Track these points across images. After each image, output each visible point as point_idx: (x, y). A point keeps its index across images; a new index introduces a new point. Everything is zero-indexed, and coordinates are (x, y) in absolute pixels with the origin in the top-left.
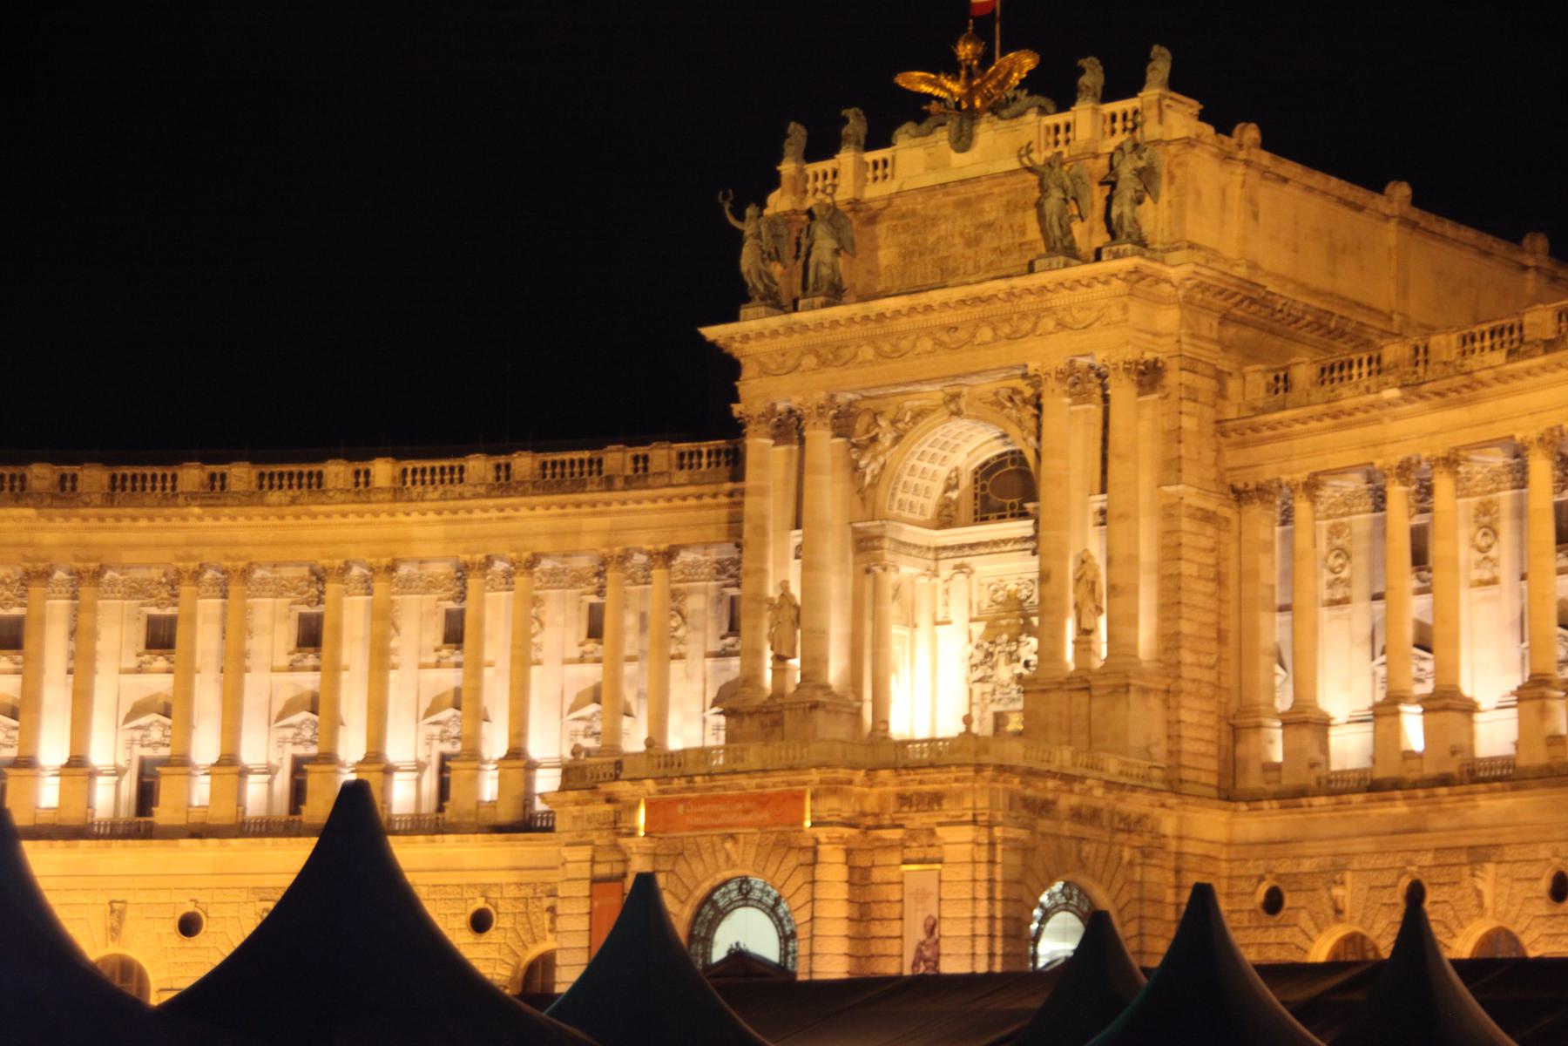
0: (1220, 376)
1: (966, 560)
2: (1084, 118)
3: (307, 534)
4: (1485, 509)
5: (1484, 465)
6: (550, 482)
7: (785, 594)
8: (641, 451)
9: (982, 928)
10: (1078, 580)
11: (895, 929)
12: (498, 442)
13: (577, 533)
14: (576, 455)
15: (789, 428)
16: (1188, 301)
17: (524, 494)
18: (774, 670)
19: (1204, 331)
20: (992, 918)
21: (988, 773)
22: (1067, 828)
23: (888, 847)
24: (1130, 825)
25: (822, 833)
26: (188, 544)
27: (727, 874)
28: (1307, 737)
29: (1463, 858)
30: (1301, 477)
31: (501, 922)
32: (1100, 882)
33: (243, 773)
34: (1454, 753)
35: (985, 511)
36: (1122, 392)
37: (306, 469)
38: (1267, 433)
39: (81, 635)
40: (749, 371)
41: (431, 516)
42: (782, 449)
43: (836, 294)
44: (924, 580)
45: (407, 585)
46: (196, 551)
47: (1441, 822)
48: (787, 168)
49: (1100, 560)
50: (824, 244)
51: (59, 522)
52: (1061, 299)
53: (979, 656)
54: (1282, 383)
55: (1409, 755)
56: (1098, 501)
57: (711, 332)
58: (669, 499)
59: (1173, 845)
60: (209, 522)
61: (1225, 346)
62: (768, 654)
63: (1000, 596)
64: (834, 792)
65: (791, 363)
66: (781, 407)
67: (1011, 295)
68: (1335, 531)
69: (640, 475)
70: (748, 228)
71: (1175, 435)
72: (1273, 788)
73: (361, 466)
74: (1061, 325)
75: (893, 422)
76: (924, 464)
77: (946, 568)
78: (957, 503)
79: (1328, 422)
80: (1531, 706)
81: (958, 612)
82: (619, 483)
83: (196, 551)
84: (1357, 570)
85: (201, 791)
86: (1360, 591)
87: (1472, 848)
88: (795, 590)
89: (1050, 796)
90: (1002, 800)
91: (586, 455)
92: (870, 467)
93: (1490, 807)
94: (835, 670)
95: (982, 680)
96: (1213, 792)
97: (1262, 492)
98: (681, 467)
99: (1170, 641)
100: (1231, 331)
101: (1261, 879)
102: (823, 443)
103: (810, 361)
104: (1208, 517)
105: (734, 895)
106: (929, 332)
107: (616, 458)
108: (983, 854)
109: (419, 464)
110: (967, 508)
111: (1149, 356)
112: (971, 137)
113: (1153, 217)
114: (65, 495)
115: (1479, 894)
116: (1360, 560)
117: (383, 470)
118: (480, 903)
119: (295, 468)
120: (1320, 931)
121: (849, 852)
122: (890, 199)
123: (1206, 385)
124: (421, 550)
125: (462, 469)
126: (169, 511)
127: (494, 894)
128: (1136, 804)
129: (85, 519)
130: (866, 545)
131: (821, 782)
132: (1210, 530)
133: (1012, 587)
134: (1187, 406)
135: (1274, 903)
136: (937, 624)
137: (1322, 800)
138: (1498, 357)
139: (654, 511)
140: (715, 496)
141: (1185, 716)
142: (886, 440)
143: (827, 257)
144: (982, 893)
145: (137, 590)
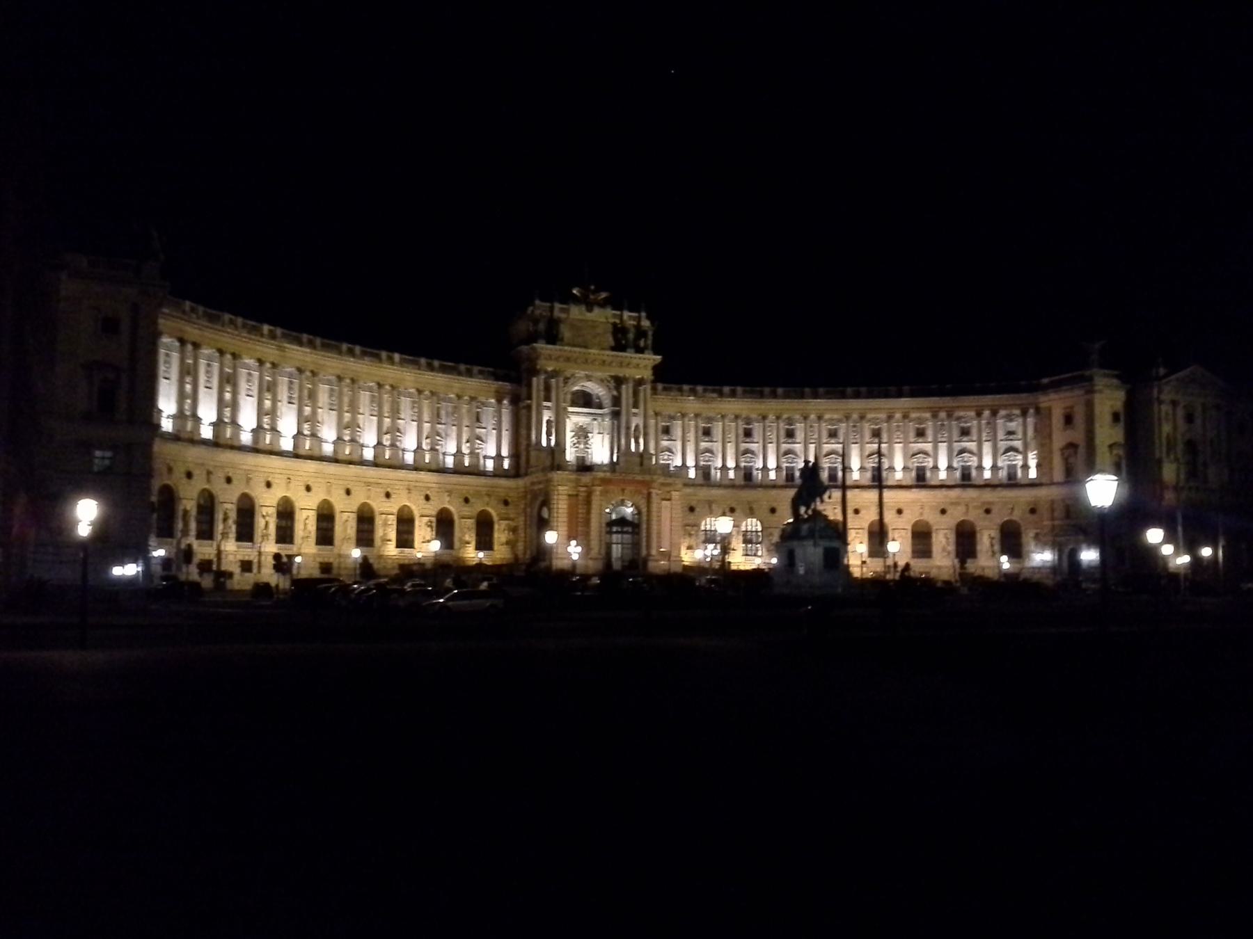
2: (626, 314)
6: (444, 370)
8: (468, 366)
10: (635, 430)
26: (344, 369)
40: (542, 357)
63: (578, 426)
69: (469, 374)
107: (462, 367)
117: (397, 356)
118: (428, 492)
133: (581, 424)
138: (715, 395)
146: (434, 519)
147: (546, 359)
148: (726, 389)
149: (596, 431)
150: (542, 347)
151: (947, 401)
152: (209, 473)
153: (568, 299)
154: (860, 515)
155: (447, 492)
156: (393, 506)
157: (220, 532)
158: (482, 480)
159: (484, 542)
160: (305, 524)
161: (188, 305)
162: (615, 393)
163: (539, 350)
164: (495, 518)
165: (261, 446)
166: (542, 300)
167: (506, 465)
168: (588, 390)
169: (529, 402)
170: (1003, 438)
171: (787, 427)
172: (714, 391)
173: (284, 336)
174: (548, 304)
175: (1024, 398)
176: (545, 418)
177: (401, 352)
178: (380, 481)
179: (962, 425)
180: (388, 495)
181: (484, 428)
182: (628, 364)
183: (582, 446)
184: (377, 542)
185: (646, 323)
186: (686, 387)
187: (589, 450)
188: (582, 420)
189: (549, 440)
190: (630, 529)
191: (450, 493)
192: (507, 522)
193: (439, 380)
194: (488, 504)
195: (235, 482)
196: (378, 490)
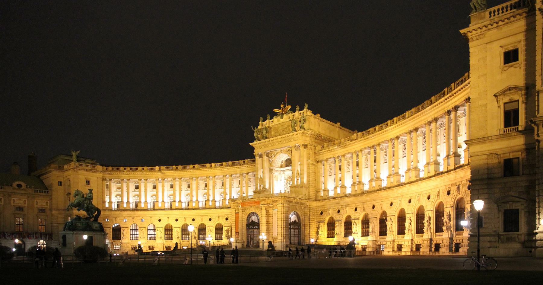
0: (315, 146)
1: (284, 172)
3: (206, 173)
4: (348, 162)
5: (348, 156)
6: (234, 165)
7: (261, 177)
8: (244, 160)
9: (283, 217)
11: (272, 218)
12: (227, 161)
13: (236, 171)
14: (236, 161)
15: (261, 156)
16: (310, 136)
17: (230, 167)
18: (260, 187)
19: (313, 140)
20: (284, 216)
21: (283, 197)
22: (294, 204)
23: (271, 207)
24: (303, 204)
25: (262, 206)
26: (191, 175)
27: (251, 212)
28: (326, 192)
29: (344, 206)
30: (325, 159)
31: (229, 219)
32: (299, 211)
33: (199, 202)
34: (344, 193)
35: (286, 165)
36: (302, 148)
37: (204, 165)
38: (321, 153)
39: (180, 186)
40: (256, 149)
41: (219, 170)
42: (260, 159)
43: (266, 138)
44: (278, 175)
45: (217, 179)
46: (192, 175)
47: (342, 202)
48: (260, 123)
49: (299, 170)
50: (265, 132)
51: (176, 173)
52: (294, 136)
53: (286, 184)
54: (323, 147)
55: (338, 194)
56: (299, 163)
57: (251, 144)
58: (248, 166)
59: (309, 207)
60: (193, 172)
61: (315, 142)
62: (259, 185)
64: (264, 201)
65: (261, 147)
66: (260, 153)
67: (287, 136)
68: (330, 166)
69: (244, 164)
70: (255, 131)
71: (309, 154)
72: (322, 199)
73: (211, 164)
74: (294, 140)
75: (274, 154)
76: (278, 160)
77: (281, 173)
78: (283, 165)
79: (328, 151)
80: (353, 187)
81: (283, 179)
82: (241, 164)
83: (192, 175)
84: (333, 171)
85: (194, 204)
86: (333, 174)
87: (346, 205)
88: (262, 176)
89: (292, 200)
90: (285, 201)
91: (237, 161)
93: (348, 200)
94: (267, 187)
95: (286, 187)
96: (314, 200)
97: (321, 161)
98: (249, 162)
99: (308, 181)
100: (316, 141)
101: (320, 210)
102: (265, 157)
103: (263, 147)
104: (313, 165)
105: (252, 214)
106: (277, 142)
108: (283, 208)
109: (217, 164)
110: (284, 165)
111: (305, 144)
112: (283, 117)
113: (305, 126)
114: (177, 169)
115: (346, 211)
116: (333, 170)
117: (213, 164)
118: (227, 217)
119: (203, 165)
120: (327, 217)
121: (266, 208)
122: (273, 126)
123: (313, 148)
124: (218, 174)
125: (223, 164)
126: (188, 171)
127: (228, 216)
128: (304, 201)
129: (179, 172)
130: (271, 170)
131: (262, 199)
132: (314, 166)
133: (290, 175)
134: (310, 150)
135: (322, 213)
136: (280, 180)
137: (328, 200)
139: (246, 168)
140: (253, 166)
141: (310, 190)
142: (273, 157)
143: (265, 133)
144: (283, 213)
145: (186, 181)
161: (122, 168)
173: (166, 169)
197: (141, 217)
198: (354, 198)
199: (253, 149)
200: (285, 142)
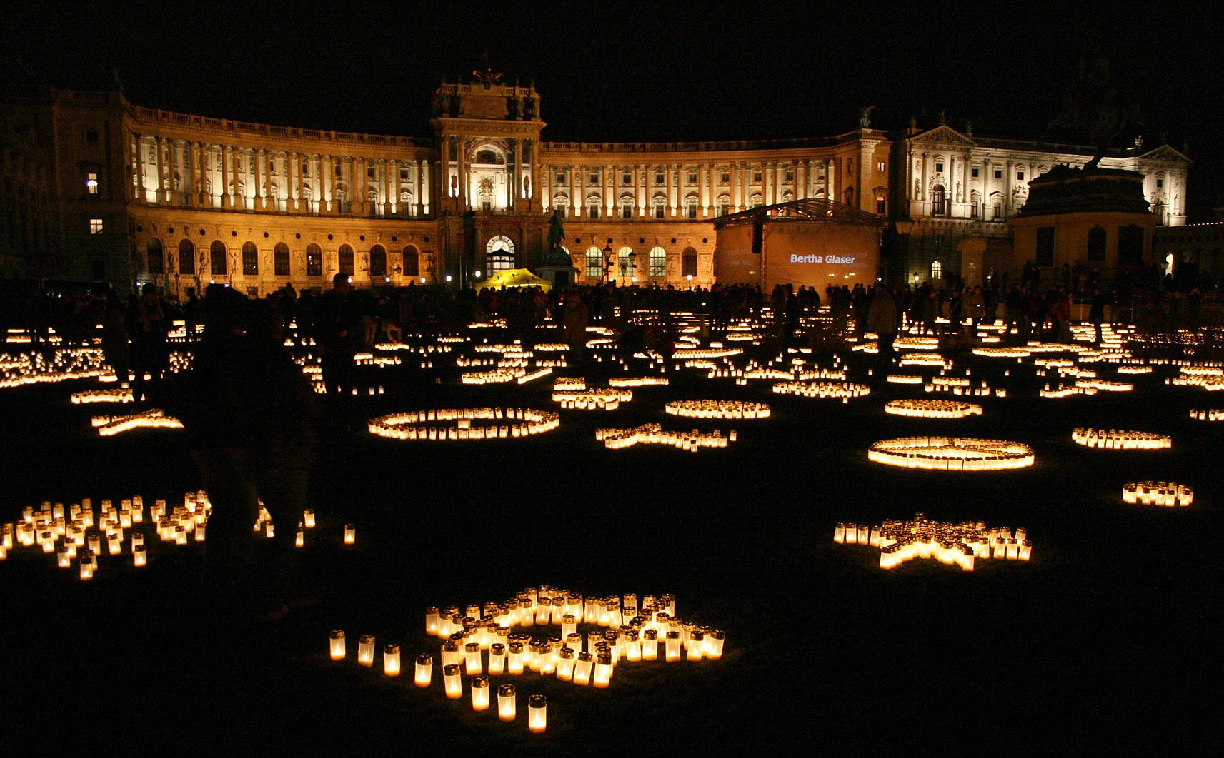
2: (518, 90)
6: (374, 141)
14: (377, 136)
48: (444, 84)
55: (577, 217)
69: (394, 142)
91: (379, 136)
92: (469, 151)
107: (388, 137)
110: (476, 161)
115: (593, 241)
117: (333, 133)
118: (363, 234)
130: (468, 167)
138: (596, 150)
146: (369, 254)
147: (449, 129)
148: (606, 145)
149: (499, 181)
150: (445, 119)
151: (772, 153)
152: (186, 228)
153: (468, 80)
154: (708, 243)
155: (379, 232)
156: (336, 245)
157: (199, 268)
158: (405, 223)
159: (411, 269)
160: (266, 261)
162: (509, 152)
163: (443, 122)
164: (419, 252)
165: (226, 207)
166: (448, 82)
167: (426, 210)
168: (491, 150)
169: (439, 162)
170: (816, 182)
171: (658, 174)
172: (595, 147)
174: (453, 85)
175: (826, 150)
176: (451, 175)
177: (336, 130)
178: (323, 227)
179: (788, 171)
180: (330, 237)
181: (412, 183)
182: (518, 129)
183: (487, 194)
184: (324, 271)
185: (535, 96)
186: (573, 144)
187: (493, 197)
188: (488, 174)
189: (454, 192)
190: (507, 258)
191: (381, 233)
192: (428, 254)
193: (369, 150)
194: (411, 241)
195: (207, 233)
196: (322, 234)
197: (200, 225)
198: (608, 226)
199: (440, 128)
200: (506, 130)
